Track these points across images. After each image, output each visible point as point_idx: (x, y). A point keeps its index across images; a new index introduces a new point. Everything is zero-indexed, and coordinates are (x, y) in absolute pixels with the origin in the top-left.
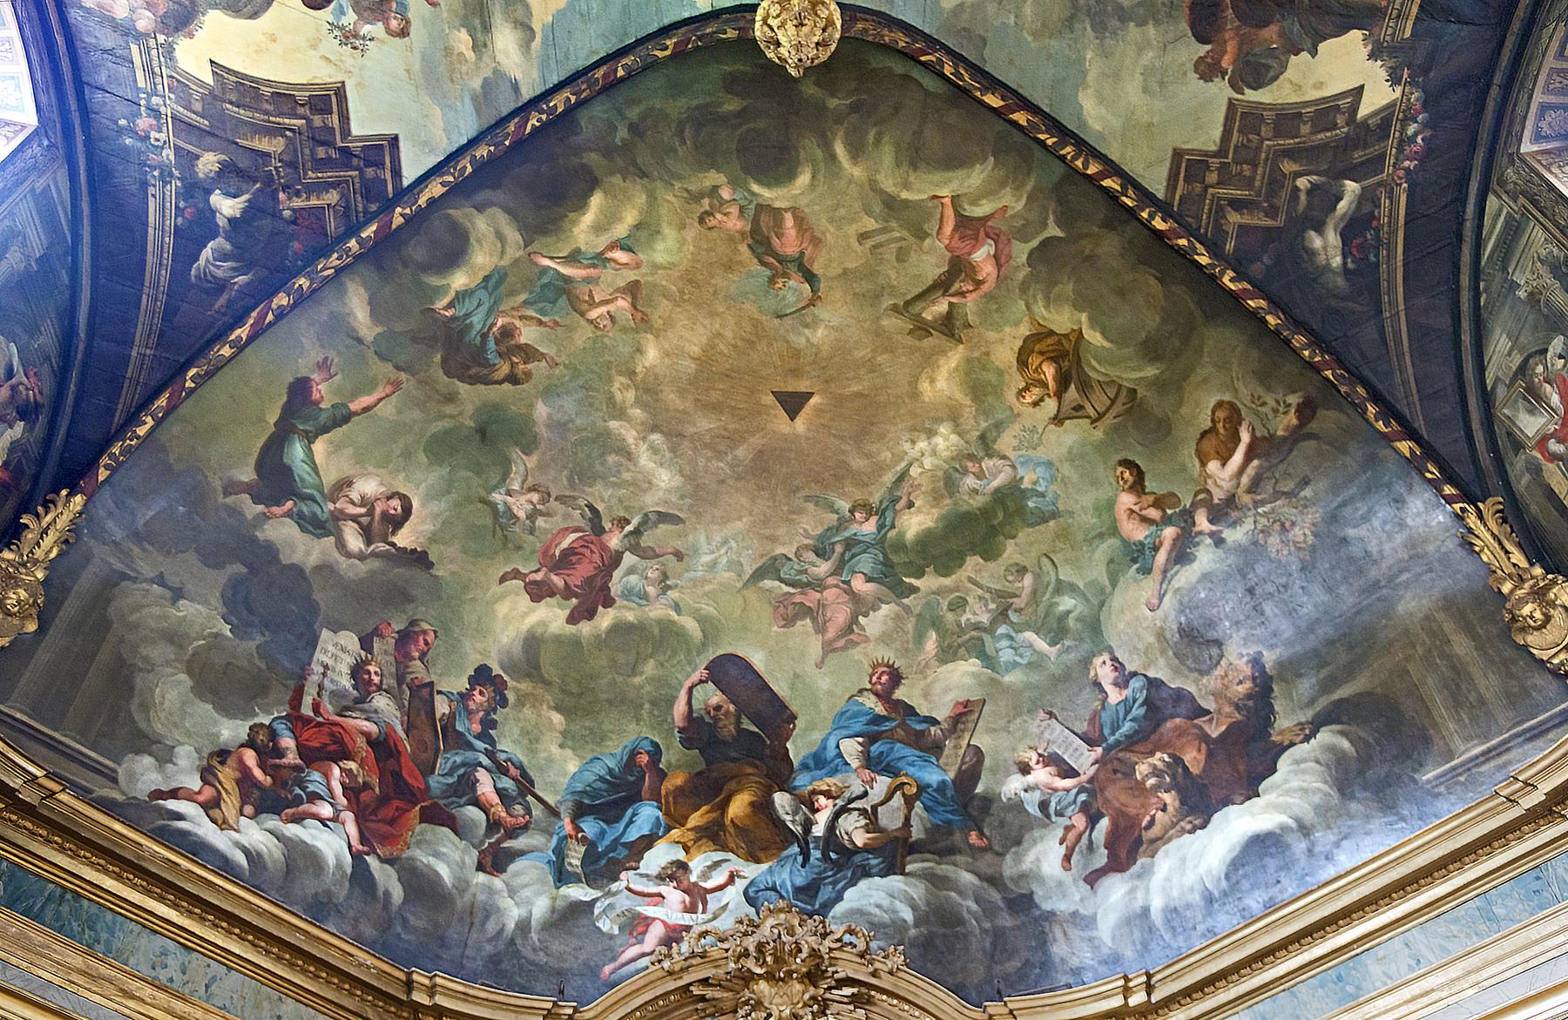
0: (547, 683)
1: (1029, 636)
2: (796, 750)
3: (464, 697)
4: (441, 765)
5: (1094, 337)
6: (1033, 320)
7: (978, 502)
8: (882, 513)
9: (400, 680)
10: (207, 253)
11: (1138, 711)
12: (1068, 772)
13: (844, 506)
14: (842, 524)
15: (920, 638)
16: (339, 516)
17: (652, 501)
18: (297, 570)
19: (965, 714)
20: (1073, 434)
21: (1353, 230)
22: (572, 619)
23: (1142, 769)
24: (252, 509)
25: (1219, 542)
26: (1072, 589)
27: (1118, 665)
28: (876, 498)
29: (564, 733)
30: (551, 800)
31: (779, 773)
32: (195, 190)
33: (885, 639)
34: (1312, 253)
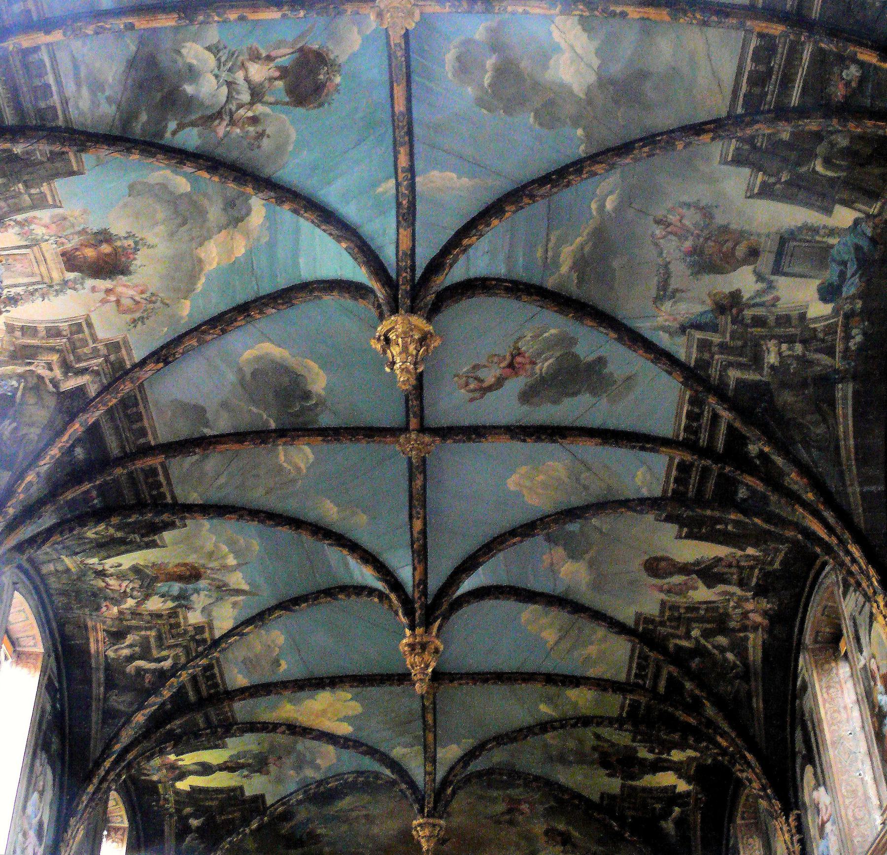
5: (576, 834)
6: (548, 825)
21: (680, 823)
32: (183, 819)
34: (662, 829)
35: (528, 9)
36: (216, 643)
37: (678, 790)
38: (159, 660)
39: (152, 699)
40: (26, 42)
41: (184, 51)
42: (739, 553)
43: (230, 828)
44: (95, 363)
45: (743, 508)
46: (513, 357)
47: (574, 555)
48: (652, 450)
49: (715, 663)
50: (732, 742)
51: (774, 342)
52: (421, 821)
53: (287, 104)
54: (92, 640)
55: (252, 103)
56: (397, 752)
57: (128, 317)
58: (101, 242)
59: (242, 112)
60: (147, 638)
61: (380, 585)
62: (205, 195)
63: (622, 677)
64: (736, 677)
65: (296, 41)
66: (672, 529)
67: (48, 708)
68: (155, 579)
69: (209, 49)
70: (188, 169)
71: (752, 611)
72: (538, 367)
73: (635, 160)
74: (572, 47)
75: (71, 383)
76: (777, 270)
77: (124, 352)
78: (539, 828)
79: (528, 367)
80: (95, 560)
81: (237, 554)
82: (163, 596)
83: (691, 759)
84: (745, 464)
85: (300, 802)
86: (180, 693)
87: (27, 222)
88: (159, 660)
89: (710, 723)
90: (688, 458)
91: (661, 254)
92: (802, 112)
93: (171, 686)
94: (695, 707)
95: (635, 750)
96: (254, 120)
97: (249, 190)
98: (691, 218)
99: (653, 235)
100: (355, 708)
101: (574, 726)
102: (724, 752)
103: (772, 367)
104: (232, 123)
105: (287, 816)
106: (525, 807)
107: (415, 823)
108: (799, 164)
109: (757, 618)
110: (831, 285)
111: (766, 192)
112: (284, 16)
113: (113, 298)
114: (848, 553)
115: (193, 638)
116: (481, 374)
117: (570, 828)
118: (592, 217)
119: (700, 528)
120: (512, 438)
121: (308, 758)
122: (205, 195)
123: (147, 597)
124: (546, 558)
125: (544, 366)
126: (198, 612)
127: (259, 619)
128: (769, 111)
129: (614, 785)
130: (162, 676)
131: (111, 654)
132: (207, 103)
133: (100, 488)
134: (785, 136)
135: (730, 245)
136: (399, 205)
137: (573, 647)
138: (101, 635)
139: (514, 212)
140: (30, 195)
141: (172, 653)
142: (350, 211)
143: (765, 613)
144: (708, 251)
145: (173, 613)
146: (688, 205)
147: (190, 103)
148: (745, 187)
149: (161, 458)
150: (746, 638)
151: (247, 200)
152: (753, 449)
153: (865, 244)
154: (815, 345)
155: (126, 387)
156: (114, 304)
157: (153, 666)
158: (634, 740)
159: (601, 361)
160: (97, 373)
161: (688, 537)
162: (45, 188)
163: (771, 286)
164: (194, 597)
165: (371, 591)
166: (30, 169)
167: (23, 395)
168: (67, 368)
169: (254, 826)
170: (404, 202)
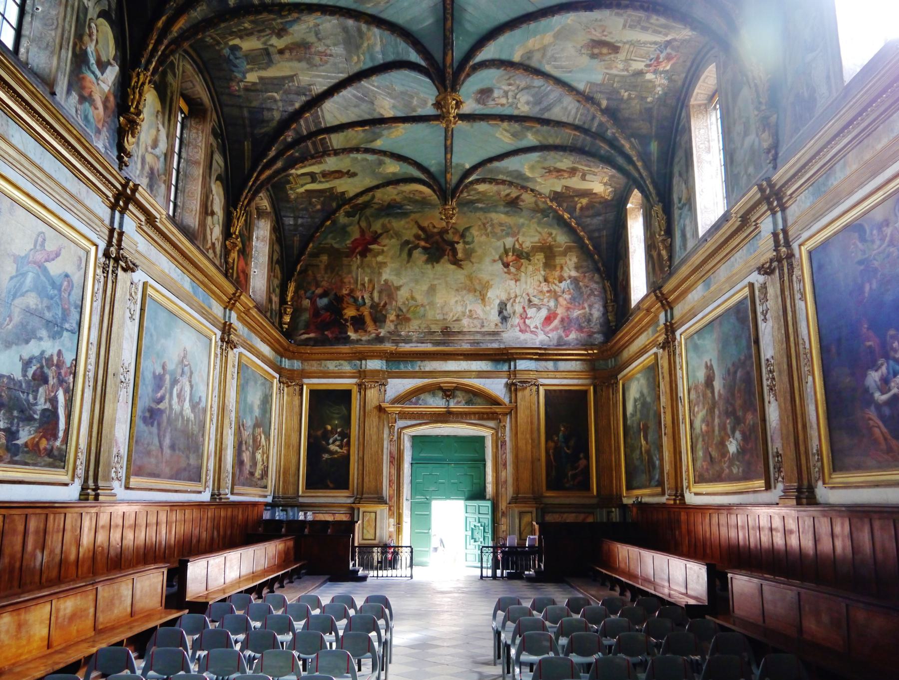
87: (623, 70)
96: (510, 85)
113: (605, 33)
163: (265, 43)
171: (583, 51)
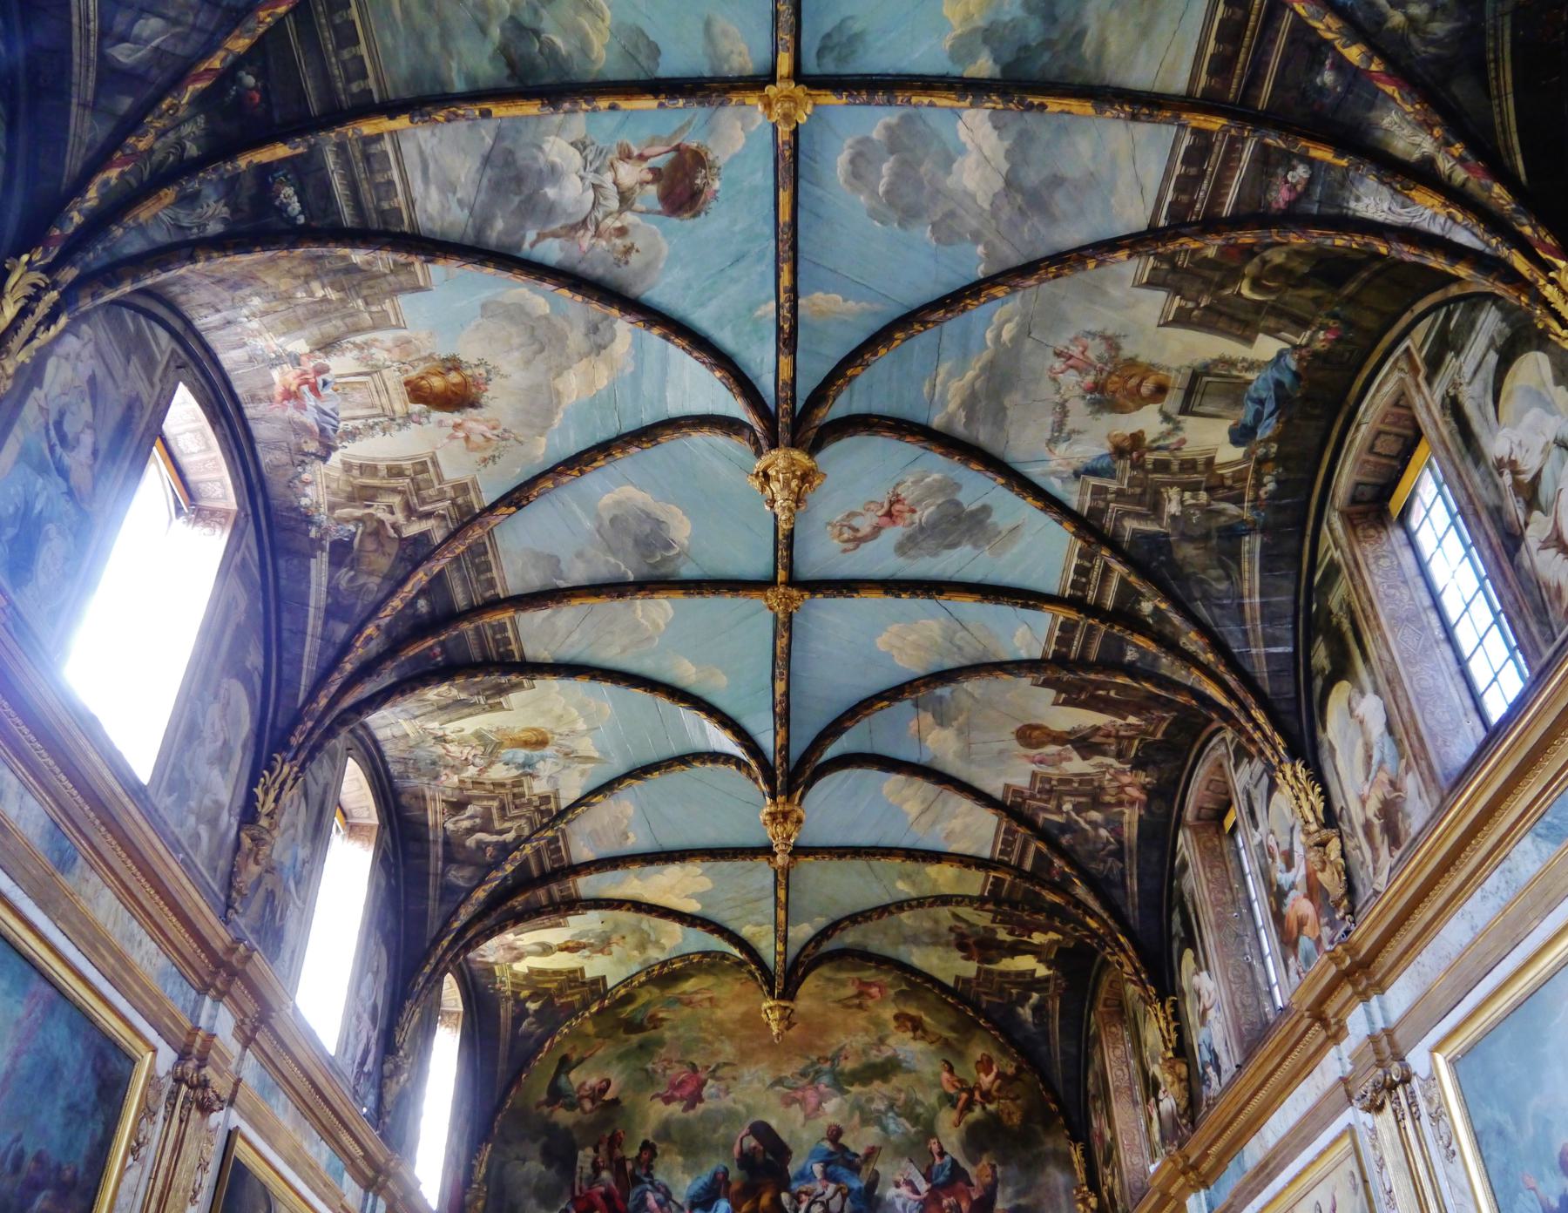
0: (673, 1142)
1: (902, 1120)
2: (793, 1169)
3: (638, 1158)
4: (632, 1197)
5: (927, 1019)
7: (879, 1060)
8: (833, 1060)
9: (611, 1159)
10: (525, 1024)
11: (947, 1172)
12: (916, 1192)
13: (814, 1058)
14: (813, 1064)
15: (851, 1116)
16: (582, 1098)
17: (721, 1059)
18: (568, 1131)
19: (872, 1153)
20: (919, 1046)
21: (1038, 1010)
22: (685, 1110)
23: (945, 1202)
24: (546, 1110)
25: (984, 1108)
26: (922, 1104)
27: (941, 1148)
28: (829, 1055)
29: (684, 1166)
30: (680, 1201)
31: (783, 1183)
32: (520, 1003)
33: (836, 1113)
35: (934, 100)
36: (562, 814)
37: (1038, 974)
38: (501, 833)
39: (494, 874)
40: (368, 128)
41: (546, 147)
42: (1120, 721)
43: (571, 1011)
44: (442, 507)
45: (1131, 670)
46: (892, 504)
47: (942, 720)
48: (1034, 607)
49: (1087, 840)
50: (1103, 922)
51: (1176, 489)
52: (772, 1003)
53: (659, 213)
54: (430, 812)
55: (620, 212)
56: (746, 931)
57: (478, 456)
58: (450, 370)
59: (609, 221)
60: (488, 809)
61: (739, 752)
62: (566, 317)
63: (986, 853)
64: (1111, 854)
65: (671, 138)
66: (1050, 694)
67: (383, 883)
68: (499, 745)
69: (573, 144)
70: (548, 287)
71: (1130, 785)
72: (916, 517)
73: (1041, 281)
74: (980, 149)
75: (413, 529)
76: (1185, 410)
77: (472, 494)
78: (888, 1013)
79: (907, 515)
80: (436, 725)
81: (587, 718)
82: (507, 764)
83: (1053, 942)
84: (1136, 624)
85: (641, 985)
86: (524, 865)
88: (501, 833)
89: (1079, 903)
90: (1073, 615)
91: (1058, 391)
92: (1238, 221)
93: (515, 859)
94: (1062, 887)
95: (994, 931)
96: (622, 232)
97: (615, 312)
98: (1096, 350)
99: (1051, 369)
100: (705, 884)
101: (931, 905)
102: (1093, 933)
103: (1173, 517)
104: (598, 234)
105: (628, 999)
106: (874, 991)
107: (765, 1005)
108: (1222, 287)
109: (1133, 792)
110: (1244, 426)
111: (1182, 320)
112: (661, 105)
113: (461, 434)
114: (1251, 719)
115: (537, 809)
116: (856, 522)
117: (922, 1014)
118: (986, 347)
119: (1079, 694)
120: (886, 593)
121: (653, 937)
122: (566, 317)
123: (491, 764)
124: (913, 724)
125: (925, 514)
126: (544, 781)
127: (607, 787)
128: (1197, 223)
129: (970, 969)
130: (505, 850)
131: (450, 826)
132: (570, 210)
133: (442, 644)
134: (1211, 252)
135: (1133, 382)
136: (779, 329)
137: (934, 823)
138: (440, 806)
139: (903, 341)
140: (370, 313)
141: (515, 824)
142: (726, 338)
143: (1143, 788)
144: (1111, 387)
145: (517, 783)
146: (1092, 335)
147: (550, 210)
148: (1158, 313)
149: (510, 613)
150: (1123, 813)
151: (611, 326)
152: (1146, 607)
153: (1287, 379)
154: (1221, 493)
155: (475, 533)
156: (463, 443)
157: (495, 838)
158: (993, 921)
159: (986, 510)
160: (443, 517)
161: (1066, 703)
162: (387, 305)
163: (1177, 428)
164: (540, 765)
165: (727, 758)
166: (371, 283)
167: (361, 541)
168: (410, 511)
169: (594, 1009)
170: (786, 326)
171: (482, 370)
